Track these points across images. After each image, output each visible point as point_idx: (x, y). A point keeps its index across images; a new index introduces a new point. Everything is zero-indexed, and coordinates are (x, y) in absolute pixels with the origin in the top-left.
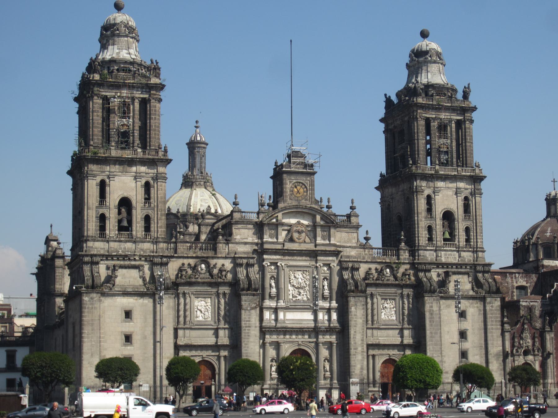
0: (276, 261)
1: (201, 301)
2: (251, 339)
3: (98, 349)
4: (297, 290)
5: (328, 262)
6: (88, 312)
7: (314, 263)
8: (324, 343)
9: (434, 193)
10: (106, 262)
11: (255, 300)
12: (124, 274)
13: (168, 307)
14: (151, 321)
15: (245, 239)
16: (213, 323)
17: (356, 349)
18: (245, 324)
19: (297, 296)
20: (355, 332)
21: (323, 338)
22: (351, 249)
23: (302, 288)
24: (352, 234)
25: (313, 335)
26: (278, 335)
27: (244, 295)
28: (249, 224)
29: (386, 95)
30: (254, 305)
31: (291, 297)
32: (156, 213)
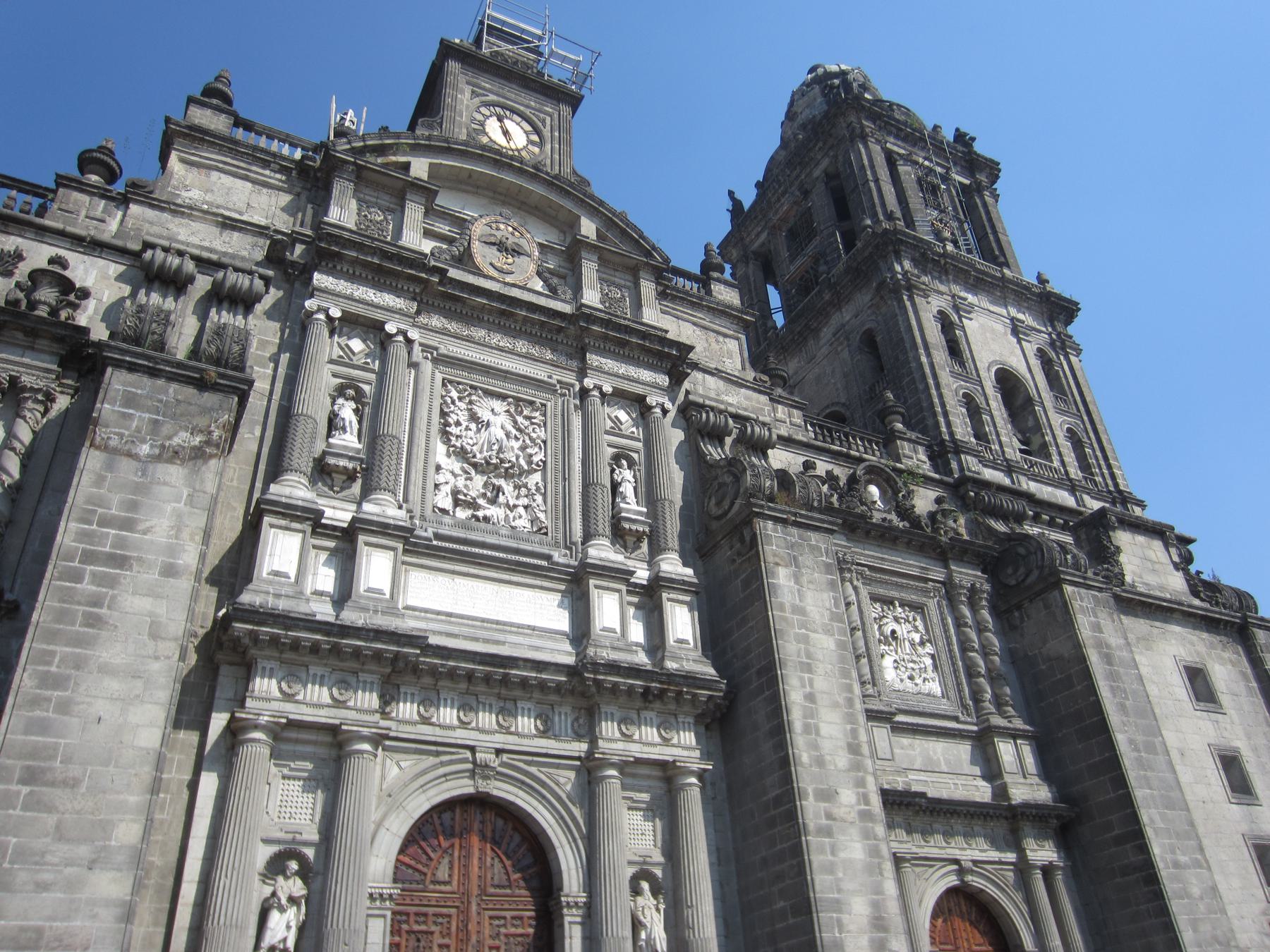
0: (378, 315)
2: (112, 652)
4: (479, 480)
5: (639, 390)
7: (570, 378)
8: (631, 768)
11: (205, 411)
15: (229, 209)
17: (827, 795)
18: (84, 536)
19: (481, 501)
20: (810, 697)
21: (627, 738)
22: (721, 383)
23: (507, 476)
24: (721, 339)
25: (564, 718)
26: (344, 684)
27: (132, 368)
28: (265, 164)
29: (731, 194)
30: (183, 438)
31: (445, 502)
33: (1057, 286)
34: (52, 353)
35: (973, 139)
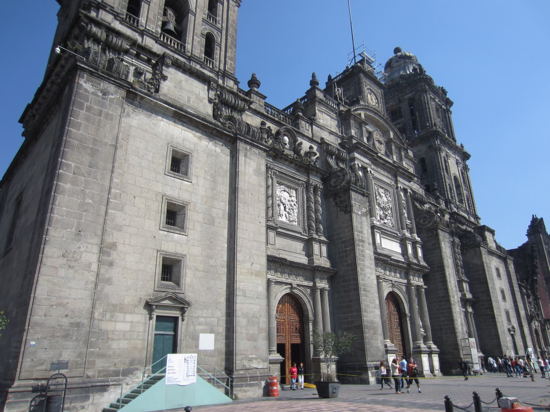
0: (365, 166)
1: (284, 191)
3: (101, 220)
5: (406, 187)
6: (87, 119)
7: (393, 183)
9: (447, 156)
10: (135, 62)
12: (180, 82)
13: (257, 172)
14: (225, 189)
16: (300, 230)
17: (454, 297)
20: (449, 274)
31: (379, 219)
32: (224, 37)
33: (466, 149)
34: (319, 177)
35: (447, 92)
